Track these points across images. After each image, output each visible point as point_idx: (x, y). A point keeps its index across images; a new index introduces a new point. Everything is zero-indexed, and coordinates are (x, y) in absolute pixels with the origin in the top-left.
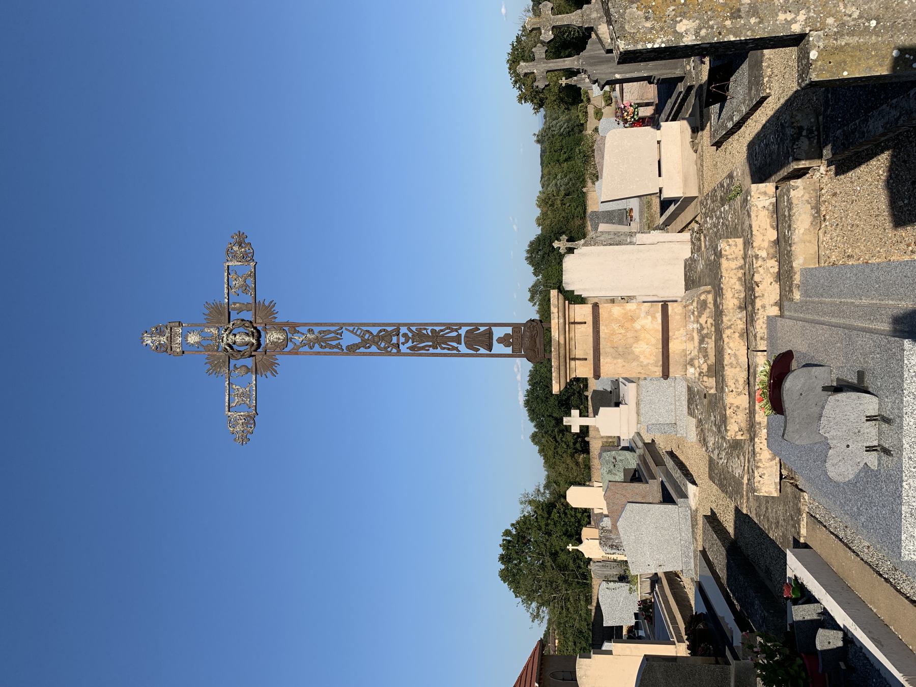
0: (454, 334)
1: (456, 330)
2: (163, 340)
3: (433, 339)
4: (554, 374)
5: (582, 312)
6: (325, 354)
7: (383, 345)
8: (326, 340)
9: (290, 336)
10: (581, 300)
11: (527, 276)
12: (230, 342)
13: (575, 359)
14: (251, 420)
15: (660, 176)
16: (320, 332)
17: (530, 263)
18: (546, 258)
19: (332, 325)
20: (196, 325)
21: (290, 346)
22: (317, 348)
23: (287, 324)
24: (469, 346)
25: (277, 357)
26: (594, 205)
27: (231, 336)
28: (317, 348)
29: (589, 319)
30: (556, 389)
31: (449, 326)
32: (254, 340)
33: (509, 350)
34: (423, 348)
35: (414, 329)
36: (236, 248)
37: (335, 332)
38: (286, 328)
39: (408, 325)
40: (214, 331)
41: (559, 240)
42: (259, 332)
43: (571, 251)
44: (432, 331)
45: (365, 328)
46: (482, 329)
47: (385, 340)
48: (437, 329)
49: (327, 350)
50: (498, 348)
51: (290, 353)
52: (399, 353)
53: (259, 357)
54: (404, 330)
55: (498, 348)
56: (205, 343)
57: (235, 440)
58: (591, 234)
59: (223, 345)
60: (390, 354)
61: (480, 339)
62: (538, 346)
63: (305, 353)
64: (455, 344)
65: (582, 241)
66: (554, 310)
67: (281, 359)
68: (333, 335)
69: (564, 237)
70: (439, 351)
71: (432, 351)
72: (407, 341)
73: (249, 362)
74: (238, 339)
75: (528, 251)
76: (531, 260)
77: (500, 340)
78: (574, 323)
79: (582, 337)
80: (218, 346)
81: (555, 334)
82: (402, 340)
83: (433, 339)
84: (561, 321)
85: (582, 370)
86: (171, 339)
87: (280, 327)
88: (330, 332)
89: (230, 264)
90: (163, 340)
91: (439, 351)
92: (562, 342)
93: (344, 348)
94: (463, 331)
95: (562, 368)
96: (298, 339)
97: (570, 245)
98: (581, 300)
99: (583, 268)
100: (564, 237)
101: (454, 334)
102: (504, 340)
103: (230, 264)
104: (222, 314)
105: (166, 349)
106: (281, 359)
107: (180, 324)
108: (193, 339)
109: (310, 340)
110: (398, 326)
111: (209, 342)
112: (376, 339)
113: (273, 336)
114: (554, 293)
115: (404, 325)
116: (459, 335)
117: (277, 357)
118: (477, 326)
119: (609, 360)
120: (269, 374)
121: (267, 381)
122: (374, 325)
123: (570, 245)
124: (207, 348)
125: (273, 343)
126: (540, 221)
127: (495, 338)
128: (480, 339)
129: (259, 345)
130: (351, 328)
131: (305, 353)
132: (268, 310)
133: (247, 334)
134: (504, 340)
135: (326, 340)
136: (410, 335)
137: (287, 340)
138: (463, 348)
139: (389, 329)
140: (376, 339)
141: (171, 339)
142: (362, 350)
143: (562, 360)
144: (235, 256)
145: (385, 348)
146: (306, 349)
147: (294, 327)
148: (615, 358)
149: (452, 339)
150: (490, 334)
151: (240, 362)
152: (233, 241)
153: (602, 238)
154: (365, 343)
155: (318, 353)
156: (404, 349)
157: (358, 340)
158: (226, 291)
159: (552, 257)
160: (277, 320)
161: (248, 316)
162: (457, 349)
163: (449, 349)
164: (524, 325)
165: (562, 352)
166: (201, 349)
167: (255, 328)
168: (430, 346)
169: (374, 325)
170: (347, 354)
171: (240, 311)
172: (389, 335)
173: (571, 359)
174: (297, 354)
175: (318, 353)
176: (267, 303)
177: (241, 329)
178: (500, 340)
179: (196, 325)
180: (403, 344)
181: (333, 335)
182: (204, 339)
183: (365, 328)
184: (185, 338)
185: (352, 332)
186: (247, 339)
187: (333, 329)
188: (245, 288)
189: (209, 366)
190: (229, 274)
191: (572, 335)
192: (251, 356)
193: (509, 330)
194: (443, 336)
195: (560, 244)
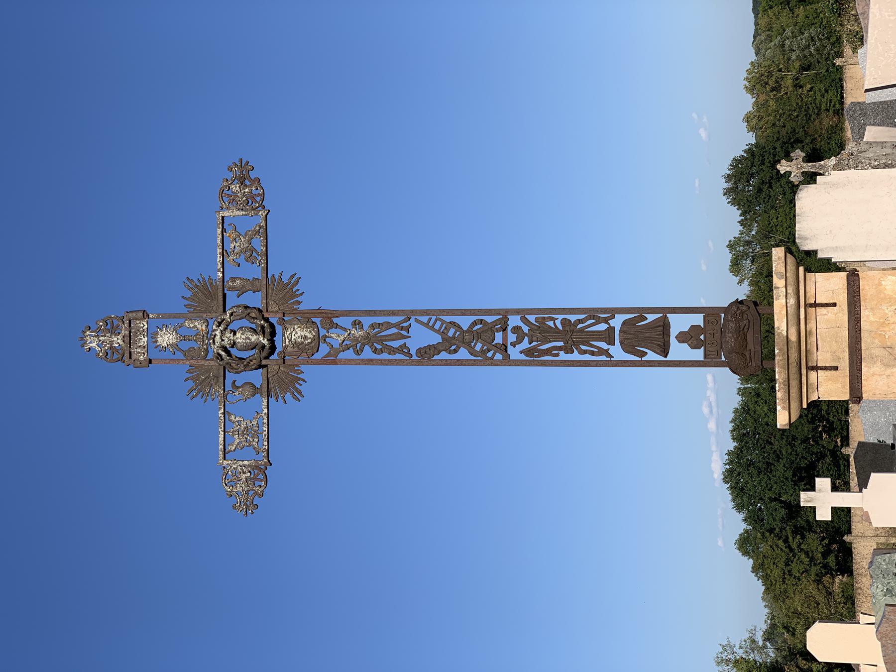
0: (602, 327)
1: (606, 321)
2: (117, 341)
3: (564, 336)
4: (779, 395)
5: (828, 287)
6: (382, 362)
7: (478, 347)
8: (382, 340)
9: (323, 332)
10: (829, 266)
11: (729, 221)
12: (226, 343)
13: (816, 368)
14: (260, 473)
15: (834, 305)
16: (373, 326)
17: (733, 202)
18: (763, 191)
19: (393, 313)
20: (171, 316)
21: (324, 349)
22: (368, 353)
23: (319, 312)
24: (627, 347)
25: (303, 368)
26: (853, 95)
27: (228, 334)
28: (368, 353)
29: (842, 298)
30: (782, 419)
31: (594, 314)
32: (264, 340)
33: (698, 354)
34: (548, 352)
35: (532, 318)
36: (235, 188)
37: (397, 325)
38: (317, 320)
39: (523, 313)
40: (200, 326)
41: (788, 157)
42: (272, 326)
43: (810, 178)
44: (565, 322)
45: (448, 319)
46: (651, 318)
47: (481, 338)
48: (573, 318)
49: (385, 356)
50: (679, 351)
51: (324, 361)
52: (507, 361)
53: (273, 369)
54: (514, 321)
55: (679, 351)
56: (185, 346)
57: (234, 507)
58: (850, 147)
59: (215, 348)
60: (491, 362)
61: (646, 335)
62: (750, 346)
63: (348, 362)
64: (603, 345)
65: (833, 161)
66: (778, 282)
67: (308, 371)
68: (394, 330)
69: (799, 154)
70: (576, 356)
71: (563, 356)
72: (520, 340)
73: (257, 377)
74: (240, 338)
75: (728, 178)
76: (735, 194)
77: (683, 337)
78: (815, 305)
79: (830, 327)
80: (207, 351)
81: (780, 324)
82: (512, 337)
83: (564, 336)
84: (792, 301)
85: (830, 388)
86: (129, 340)
87: (306, 319)
88: (389, 325)
89: (226, 214)
90: (117, 341)
91: (576, 356)
92: (793, 338)
93: (413, 352)
94: (617, 322)
95: (794, 383)
96: (336, 337)
97: (809, 167)
98: (829, 266)
99: (834, 209)
100: (799, 154)
101: (602, 327)
102: (690, 337)
103: (226, 214)
104: (210, 298)
105: (124, 355)
106: (308, 371)
107: (145, 315)
108: (165, 338)
109: (356, 340)
110: (505, 314)
111: (193, 344)
112: (467, 337)
113: (296, 334)
114: (778, 253)
115: (516, 312)
116: (611, 329)
117: (303, 368)
118: (641, 312)
119: (877, 368)
120: (288, 396)
121: (285, 409)
122: (464, 313)
123: (809, 167)
124: (189, 354)
125: (295, 344)
126: (753, 121)
127: (674, 332)
128: (646, 335)
129: (273, 348)
130: (425, 319)
131: (348, 362)
132: (284, 291)
133: (255, 331)
134: (690, 337)
135: (382, 340)
136: (526, 329)
137: (318, 340)
138: (617, 352)
139: (490, 319)
140: (467, 337)
141: (129, 340)
142: (444, 355)
143: (793, 369)
144: (233, 200)
145: (483, 352)
146: (350, 354)
147: (329, 318)
148: (887, 366)
149: (599, 336)
150: (664, 326)
151: (242, 378)
152: (230, 176)
153: (870, 155)
154: (448, 344)
155: (370, 362)
156: (515, 353)
157: (436, 339)
158: (219, 259)
159: (777, 188)
160: (302, 307)
161: (255, 300)
162: (606, 353)
163: (592, 353)
164: (726, 310)
165: (793, 355)
166: (180, 355)
167: (267, 320)
168: (560, 348)
169: (464, 313)
170: (418, 363)
171: (242, 291)
172: (490, 329)
173: (810, 368)
174: (334, 362)
175: (370, 362)
176: (285, 279)
177: (245, 323)
178: (683, 337)
179: (171, 316)
180: (514, 345)
181: (394, 330)
182: (184, 338)
183: (448, 319)
184: (153, 337)
185: (426, 325)
186: (254, 338)
187: (394, 320)
188: (250, 253)
189: (191, 384)
190: (224, 230)
191: (811, 325)
192: (261, 366)
193: (698, 320)
194: (582, 330)
195: (792, 167)
